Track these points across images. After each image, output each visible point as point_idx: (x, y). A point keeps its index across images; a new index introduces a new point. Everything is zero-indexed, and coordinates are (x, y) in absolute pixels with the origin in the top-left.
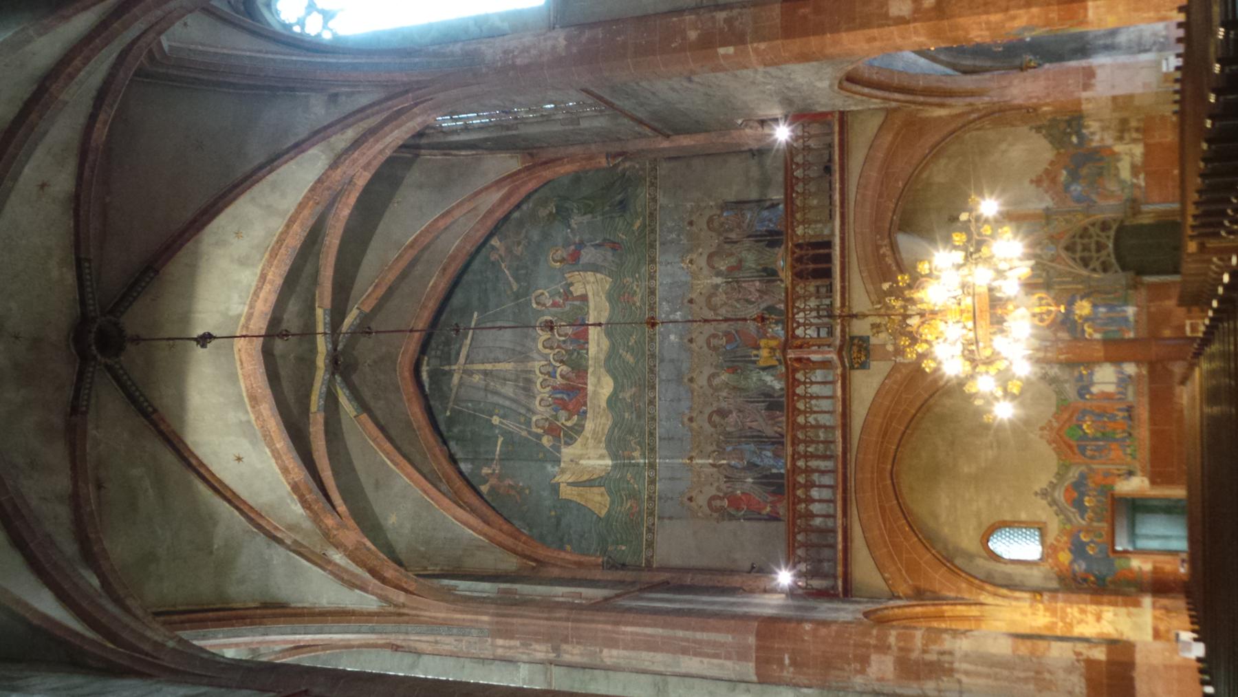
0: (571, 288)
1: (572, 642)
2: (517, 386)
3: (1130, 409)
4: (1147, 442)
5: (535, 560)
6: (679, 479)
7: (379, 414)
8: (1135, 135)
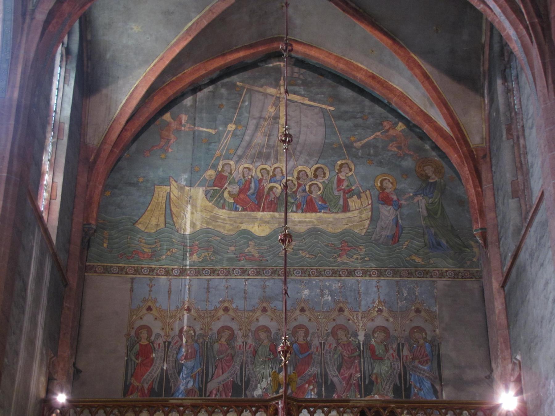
0: (355, 196)
6: (169, 298)
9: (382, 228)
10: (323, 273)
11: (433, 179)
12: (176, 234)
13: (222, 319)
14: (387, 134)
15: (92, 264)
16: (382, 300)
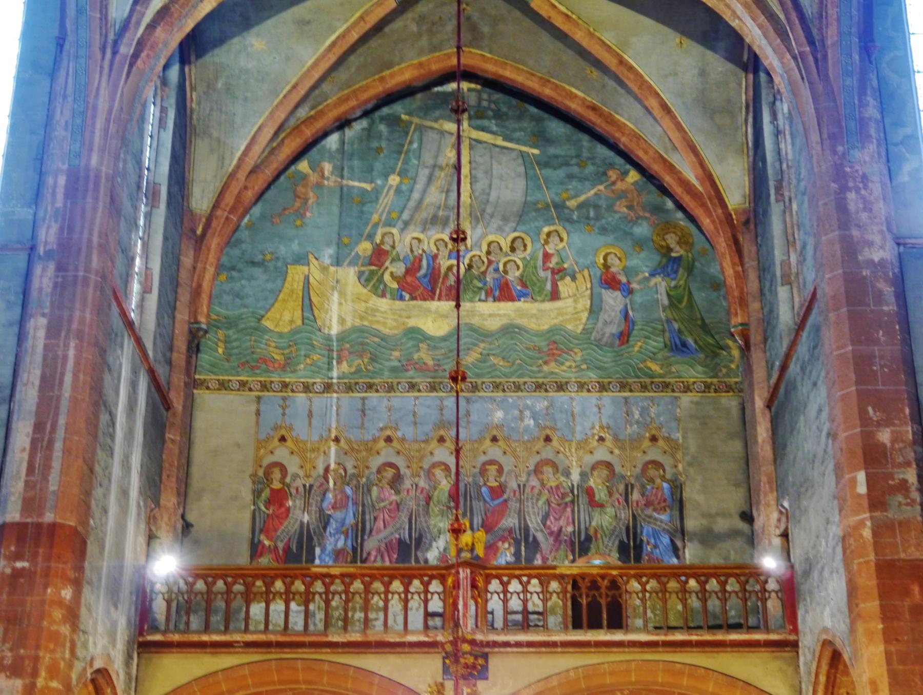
0: (568, 279)
1: (57, 277)
2: (439, 208)
7: (398, 24)
10: (522, 387)
11: (677, 252)
12: (318, 333)
13: (383, 453)
14: (613, 188)
15: (202, 377)
16: (605, 424)
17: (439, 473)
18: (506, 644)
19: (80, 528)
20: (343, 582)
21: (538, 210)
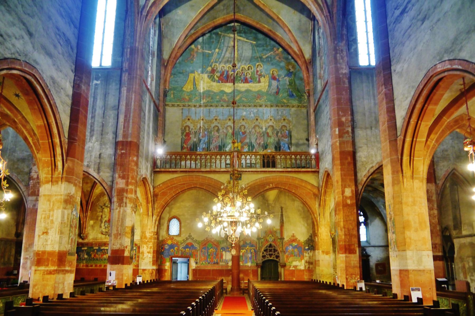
0: (263, 77)
3: (217, 263)
4: (207, 268)
5: (167, 65)
7: (218, 6)
8: (307, 267)
9: (272, 89)
13: (215, 123)
15: (168, 103)
17: (229, 128)
18: (246, 171)
19: (138, 142)
20: (205, 156)
21: (255, 59)
